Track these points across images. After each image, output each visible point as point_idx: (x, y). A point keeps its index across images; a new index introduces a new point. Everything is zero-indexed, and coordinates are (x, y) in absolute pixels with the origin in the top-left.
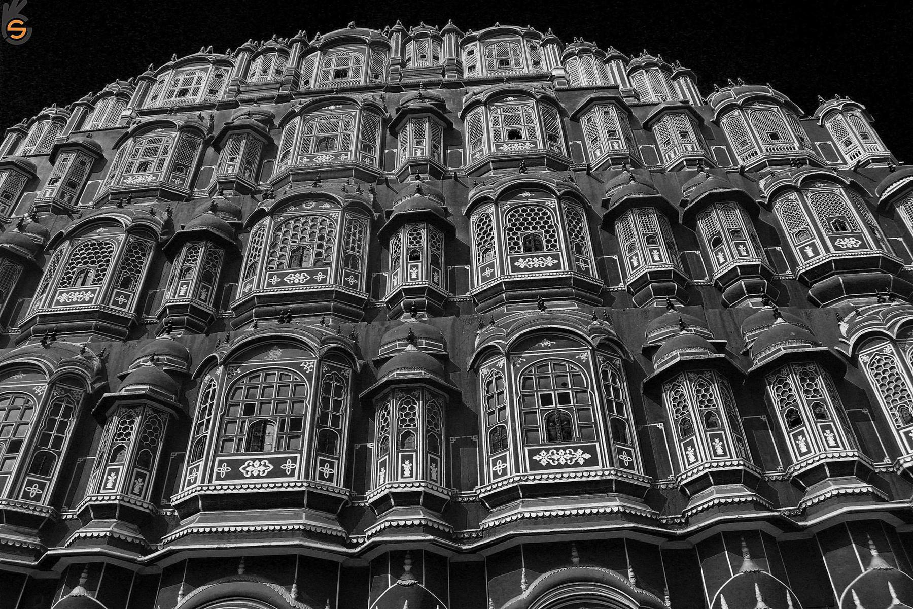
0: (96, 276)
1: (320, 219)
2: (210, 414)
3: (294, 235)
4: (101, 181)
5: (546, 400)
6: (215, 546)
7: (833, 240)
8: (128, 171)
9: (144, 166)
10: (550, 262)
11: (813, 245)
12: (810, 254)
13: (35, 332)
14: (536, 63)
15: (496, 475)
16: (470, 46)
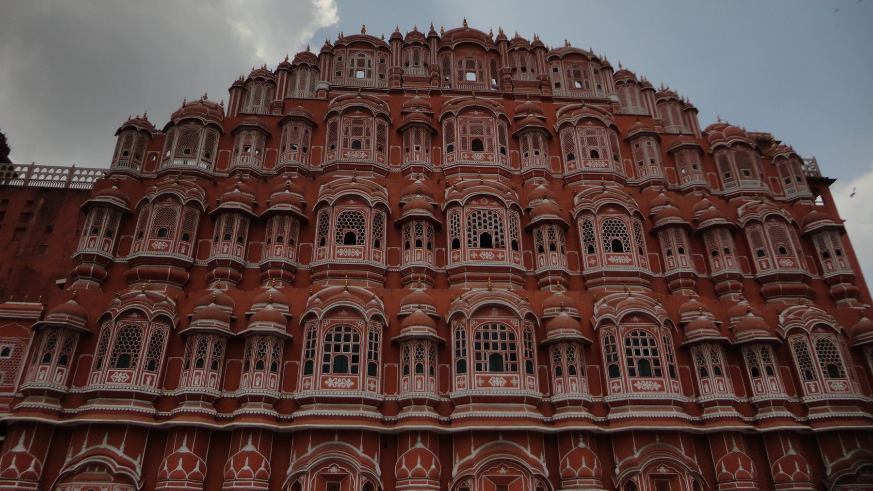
0: (360, 238)
1: (493, 213)
2: (464, 345)
3: (480, 224)
4: (322, 147)
5: (638, 352)
6: (493, 427)
7: (779, 260)
9: (357, 145)
10: (627, 260)
11: (766, 261)
12: (765, 267)
13: (331, 275)
14: (599, 87)
15: (614, 391)
16: (555, 64)
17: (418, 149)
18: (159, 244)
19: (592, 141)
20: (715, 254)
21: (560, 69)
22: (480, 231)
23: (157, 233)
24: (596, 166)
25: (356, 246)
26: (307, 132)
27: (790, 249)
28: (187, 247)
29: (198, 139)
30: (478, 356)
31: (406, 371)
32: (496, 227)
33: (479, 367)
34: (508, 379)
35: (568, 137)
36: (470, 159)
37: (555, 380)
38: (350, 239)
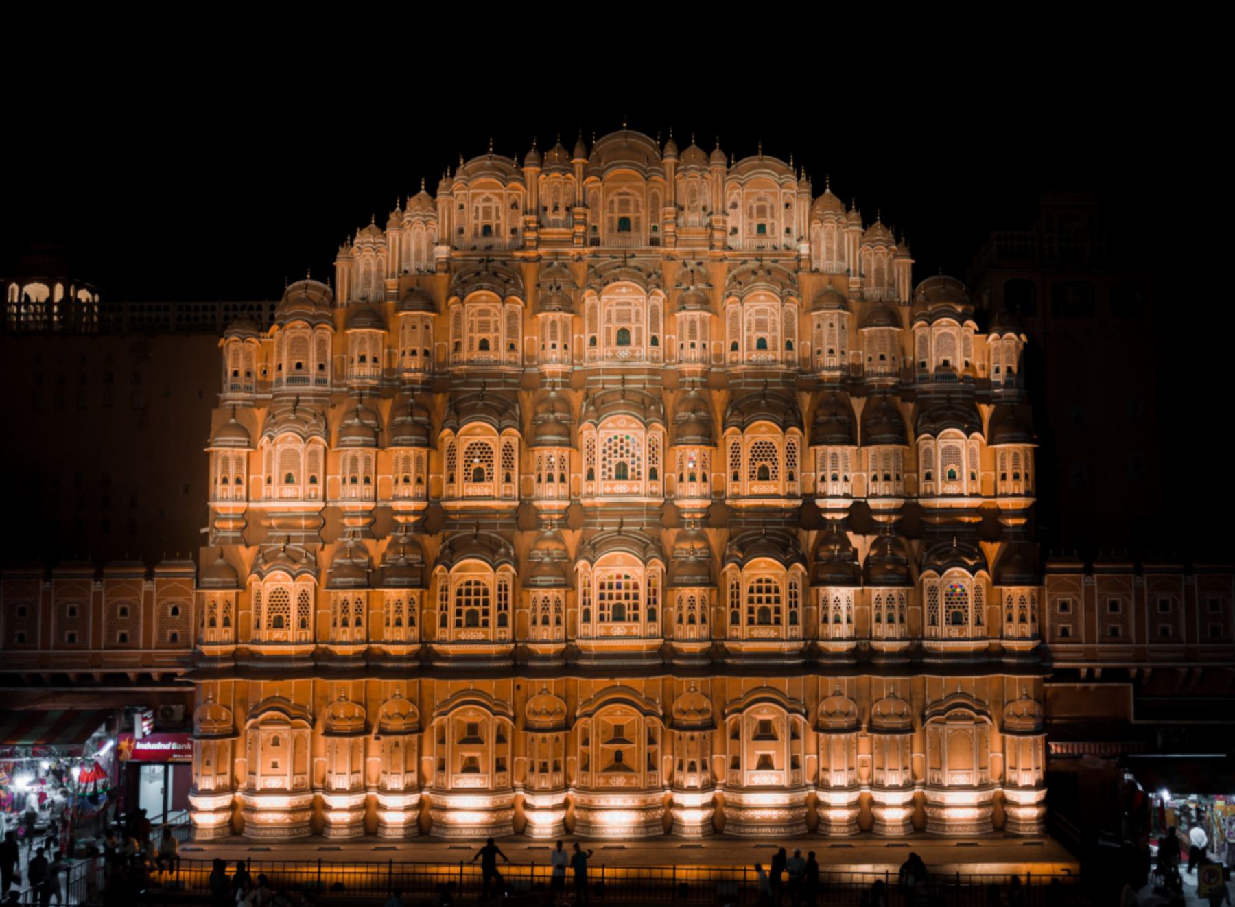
5: (760, 601)
8: (471, 347)
14: (788, 231)
17: (554, 346)
19: (761, 325)
25: (485, 483)
29: (308, 350)
30: (602, 607)
33: (602, 618)
34: (629, 628)
35: (735, 316)
38: (479, 476)
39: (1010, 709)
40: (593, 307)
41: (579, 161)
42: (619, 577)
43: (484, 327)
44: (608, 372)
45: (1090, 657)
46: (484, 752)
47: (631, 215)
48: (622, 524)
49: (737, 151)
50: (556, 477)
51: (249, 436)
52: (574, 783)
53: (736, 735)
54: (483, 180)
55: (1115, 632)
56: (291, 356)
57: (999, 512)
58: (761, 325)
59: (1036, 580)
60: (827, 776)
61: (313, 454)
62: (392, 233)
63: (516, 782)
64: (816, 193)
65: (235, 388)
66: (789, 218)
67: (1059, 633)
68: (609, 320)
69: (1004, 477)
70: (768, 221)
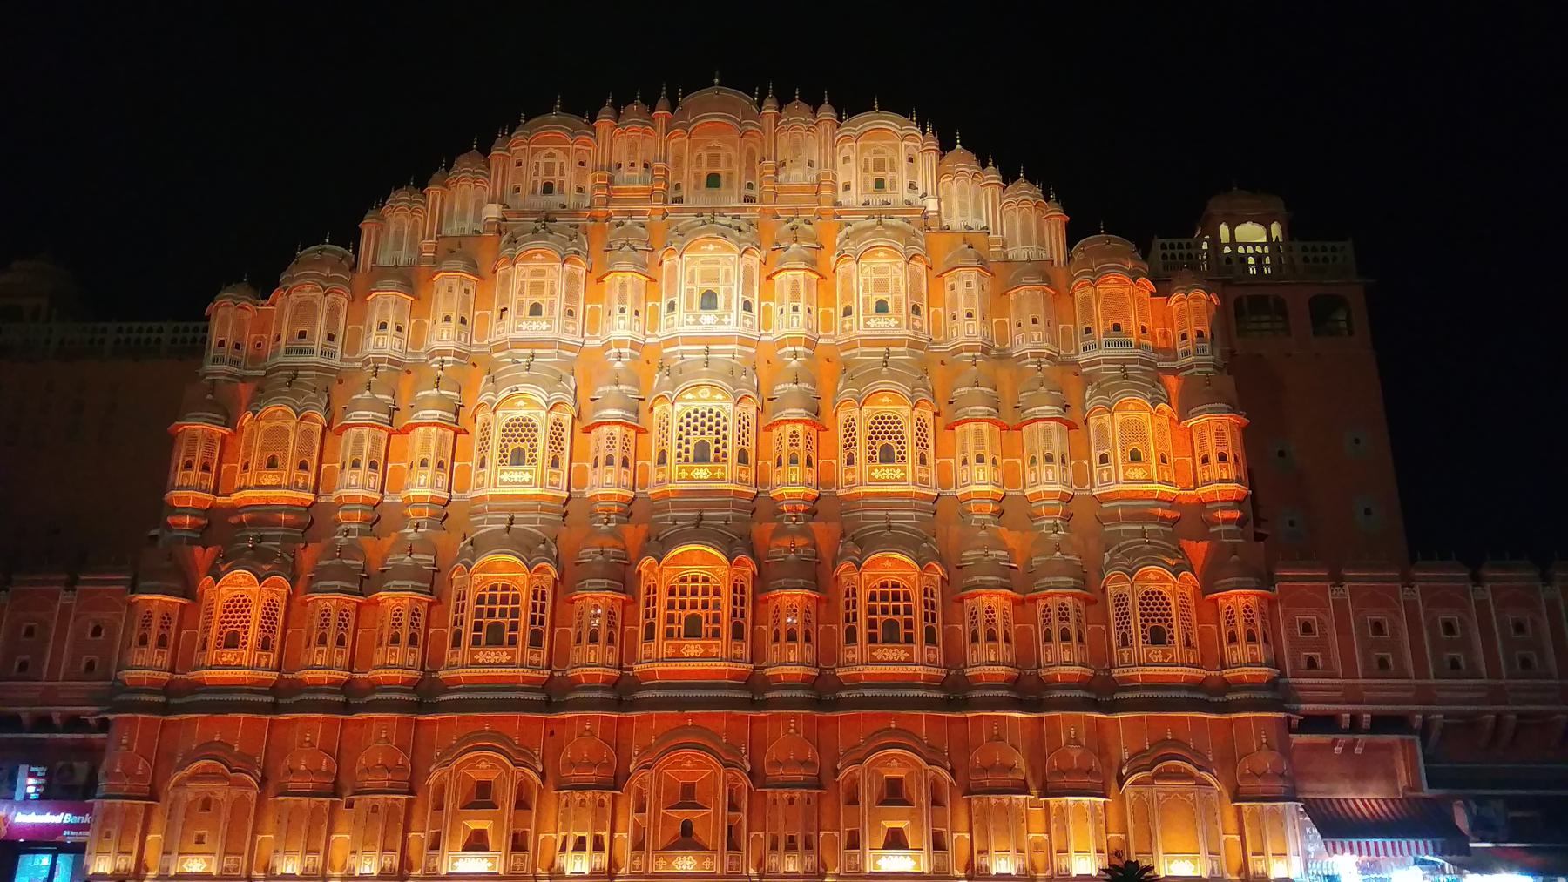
3: (695, 429)
7: (1125, 471)
8: (519, 312)
9: (536, 310)
10: (898, 474)
17: (622, 311)
18: (270, 478)
19: (880, 285)
20: (1033, 461)
21: (853, 157)
22: (695, 438)
23: (265, 461)
24: (883, 324)
25: (526, 467)
26: (467, 292)
27: (1148, 453)
28: (306, 478)
30: (671, 619)
31: (579, 641)
32: (718, 433)
33: (670, 634)
35: (847, 278)
36: (697, 323)
37: (770, 646)
38: (518, 458)
39: (1245, 766)
40: (673, 269)
41: (661, 113)
42: (695, 580)
43: (537, 288)
44: (688, 340)
45: (1353, 697)
46: (498, 822)
47: (722, 170)
48: (701, 518)
49: (850, 105)
50: (617, 460)
51: (228, 415)
52: (622, 871)
53: (853, 801)
54: (549, 133)
55: (1383, 663)
56: (293, 322)
57: (1201, 504)
58: (880, 285)
59: (1265, 580)
60: (986, 861)
61: (307, 435)
62: (433, 191)
63: (539, 871)
64: (945, 147)
65: (215, 360)
66: (913, 173)
67: (1304, 665)
68: (692, 281)
69: (1205, 460)
70: (887, 177)
